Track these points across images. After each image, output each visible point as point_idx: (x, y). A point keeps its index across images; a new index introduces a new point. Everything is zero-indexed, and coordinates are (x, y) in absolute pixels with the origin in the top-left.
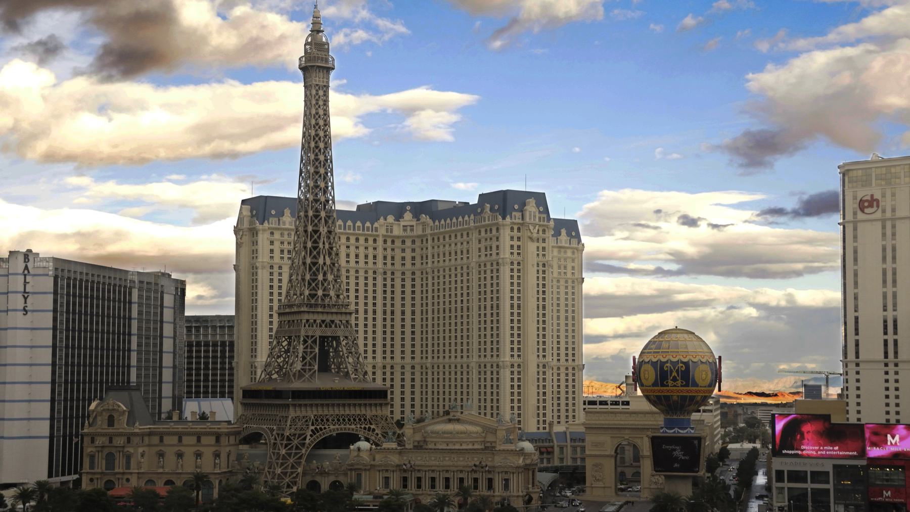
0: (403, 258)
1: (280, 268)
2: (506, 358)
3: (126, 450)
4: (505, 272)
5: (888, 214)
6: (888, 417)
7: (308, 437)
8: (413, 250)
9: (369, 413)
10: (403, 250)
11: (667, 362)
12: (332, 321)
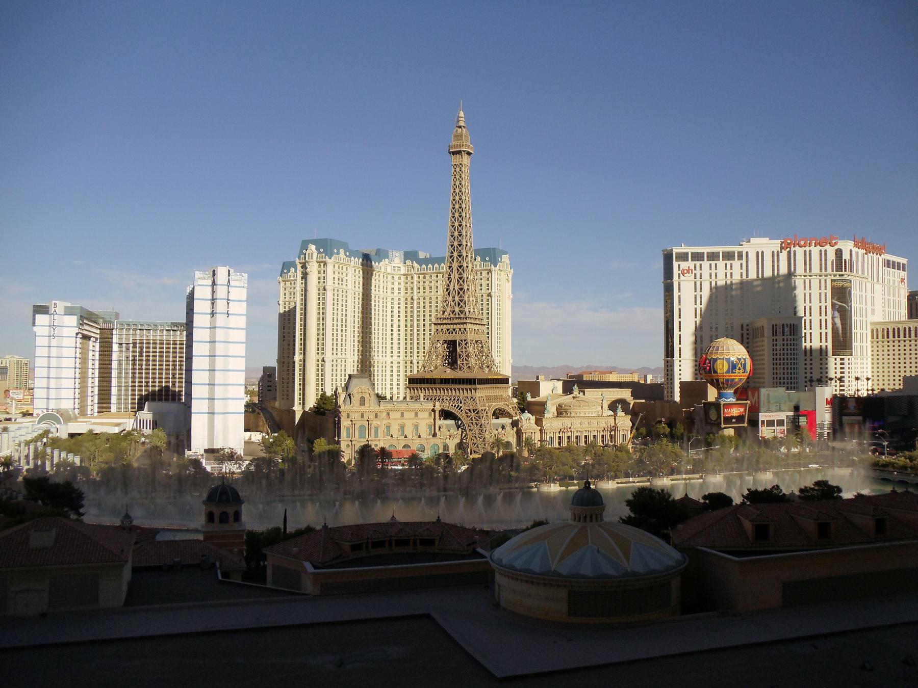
0: (393, 289)
8: (399, 284)
10: (393, 283)
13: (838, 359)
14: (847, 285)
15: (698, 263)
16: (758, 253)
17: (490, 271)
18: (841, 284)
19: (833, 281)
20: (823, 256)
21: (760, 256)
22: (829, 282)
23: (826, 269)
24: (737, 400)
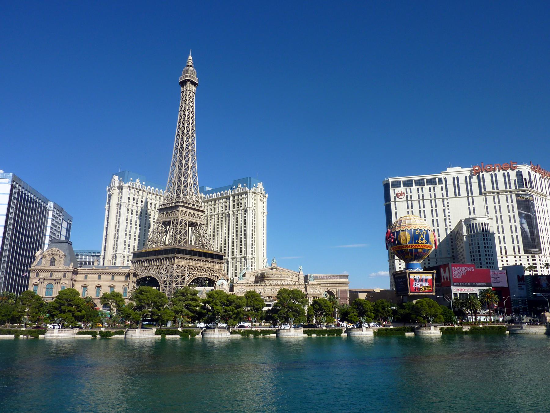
1: (132, 207)
2: (249, 254)
3: (62, 282)
4: (249, 213)
5: (409, 199)
6: (516, 262)
7: (186, 278)
9: (215, 266)
11: (417, 230)
12: (194, 214)
13: (530, 257)
14: (530, 198)
15: (408, 188)
16: (454, 178)
17: (246, 194)
18: (525, 198)
19: (517, 195)
20: (507, 178)
21: (456, 181)
22: (514, 196)
23: (510, 187)
24: (424, 270)
